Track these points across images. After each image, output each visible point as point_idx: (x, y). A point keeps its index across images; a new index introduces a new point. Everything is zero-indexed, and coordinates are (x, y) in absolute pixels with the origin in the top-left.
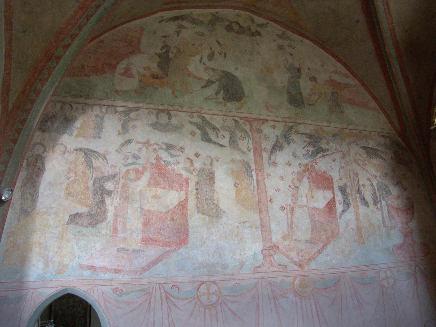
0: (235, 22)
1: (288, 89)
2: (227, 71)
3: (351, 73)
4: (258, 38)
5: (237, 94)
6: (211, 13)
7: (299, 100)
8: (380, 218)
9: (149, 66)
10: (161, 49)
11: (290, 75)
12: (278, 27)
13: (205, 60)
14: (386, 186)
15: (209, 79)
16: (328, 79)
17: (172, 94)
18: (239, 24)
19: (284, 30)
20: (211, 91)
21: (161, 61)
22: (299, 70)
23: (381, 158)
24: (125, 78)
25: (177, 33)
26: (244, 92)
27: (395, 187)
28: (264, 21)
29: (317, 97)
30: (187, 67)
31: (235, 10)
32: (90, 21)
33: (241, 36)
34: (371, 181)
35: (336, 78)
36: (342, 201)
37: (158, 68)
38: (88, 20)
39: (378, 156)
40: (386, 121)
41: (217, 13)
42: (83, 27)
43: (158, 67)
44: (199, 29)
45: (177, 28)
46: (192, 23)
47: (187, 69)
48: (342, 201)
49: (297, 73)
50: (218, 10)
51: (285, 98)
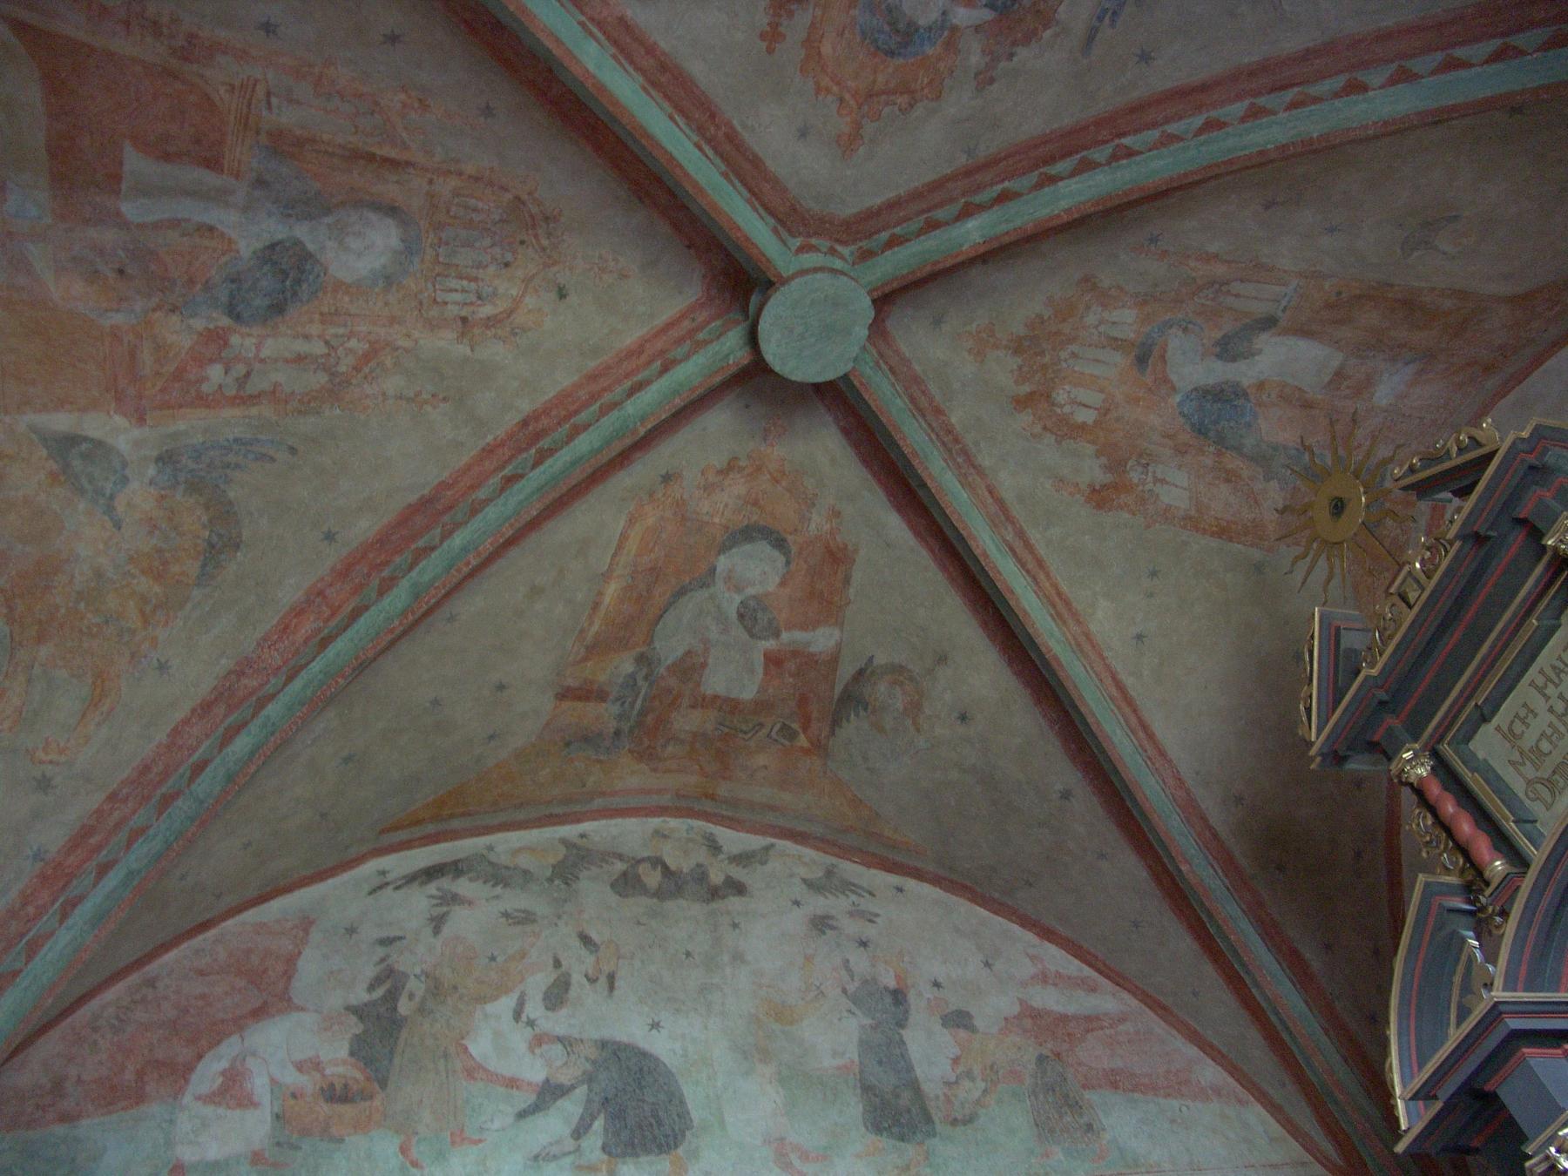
0: (649, 859)
1: (861, 1072)
2: (618, 1039)
3: (1101, 973)
4: (734, 903)
5: (660, 1124)
6: (565, 842)
7: (909, 1111)
9: (318, 1057)
10: (371, 988)
11: (867, 1021)
12: (808, 853)
13: (535, 1009)
15: (547, 1081)
16: (1016, 1009)
17: (401, 1157)
18: (665, 867)
19: (834, 860)
20: (554, 1124)
21: (365, 1032)
22: (898, 996)
24: (221, 1111)
25: (434, 924)
26: (688, 1113)
28: (756, 842)
29: (983, 1085)
30: (464, 1042)
31: (650, 820)
32: (70, 922)
33: (670, 905)
35: (1050, 1000)
37: (353, 1060)
38: (64, 915)
40: (1276, 1128)
41: (582, 836)
42: (43, 945)
43: (352, 1054)
44: (516, 900)
45: (437, 905)
46: (491, 883)
47: (466, 1049)
49: (893, 1009)
50: (586, 826)
51: (854, 1108)
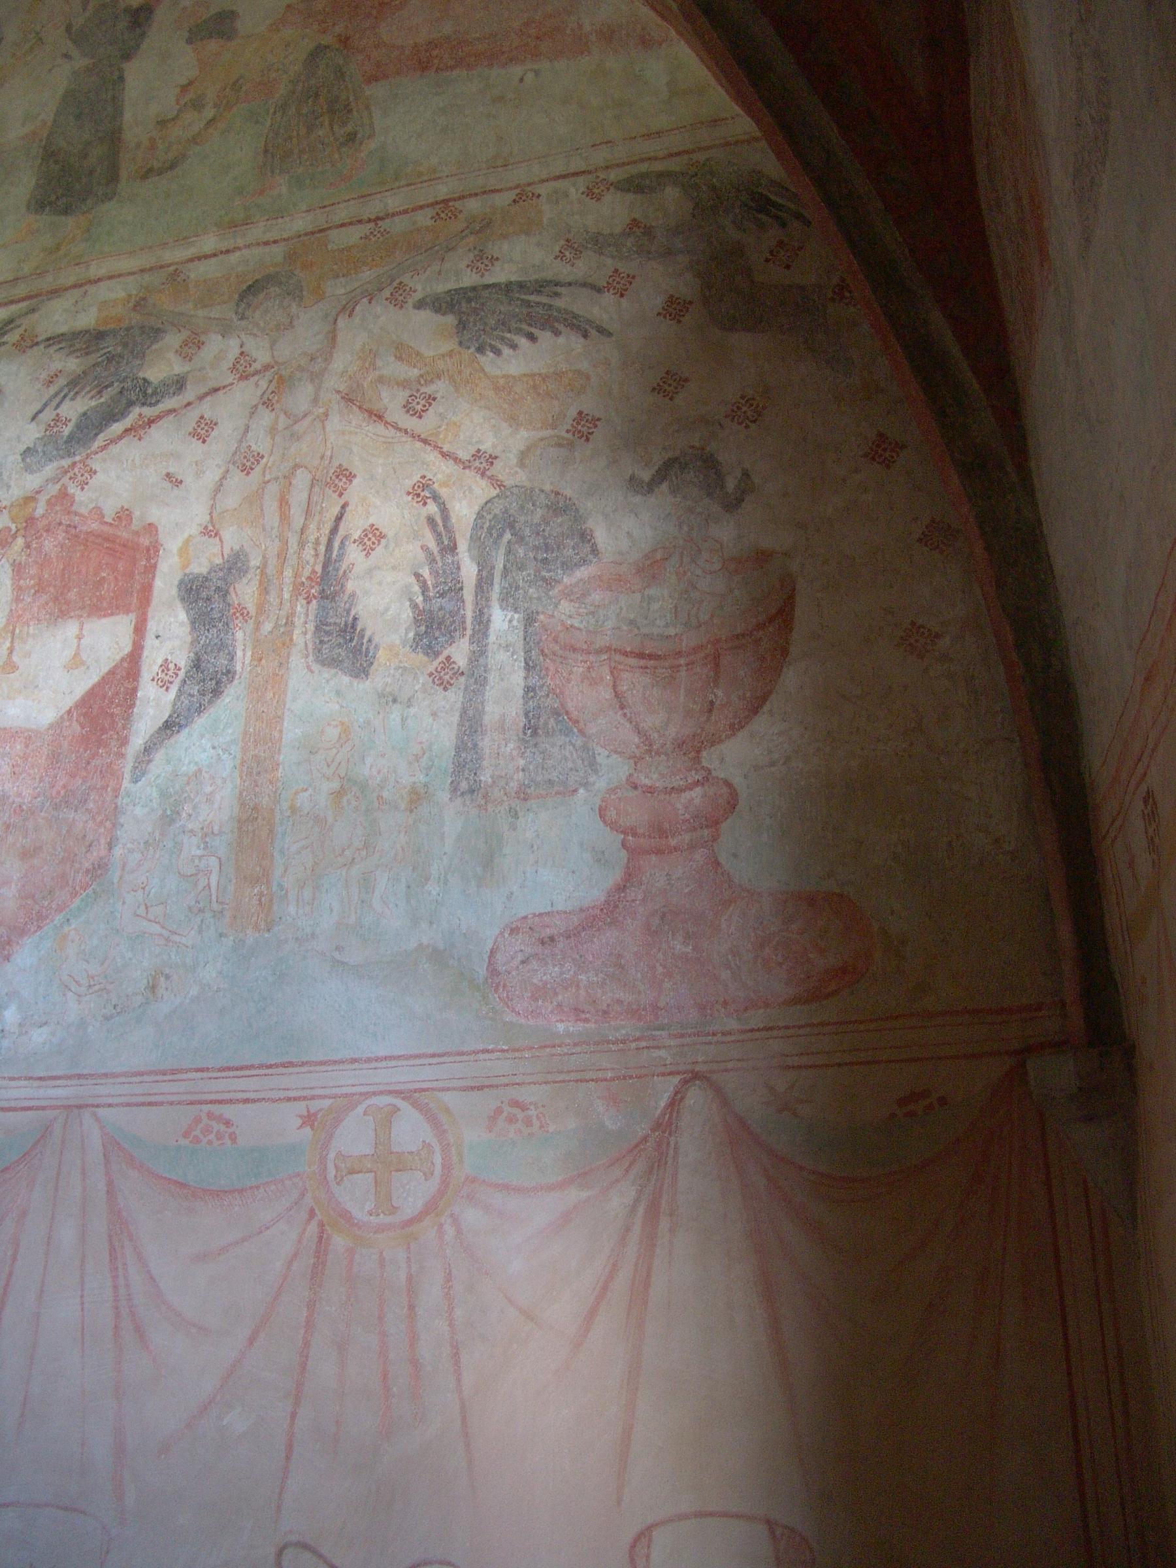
8: (445, 736)
14: (559, 506)
23: (572, 326)
27: (638, 499)
34: (436, 497)
36: (182, 664)
39: (552, 321)
48: (182, 664)
